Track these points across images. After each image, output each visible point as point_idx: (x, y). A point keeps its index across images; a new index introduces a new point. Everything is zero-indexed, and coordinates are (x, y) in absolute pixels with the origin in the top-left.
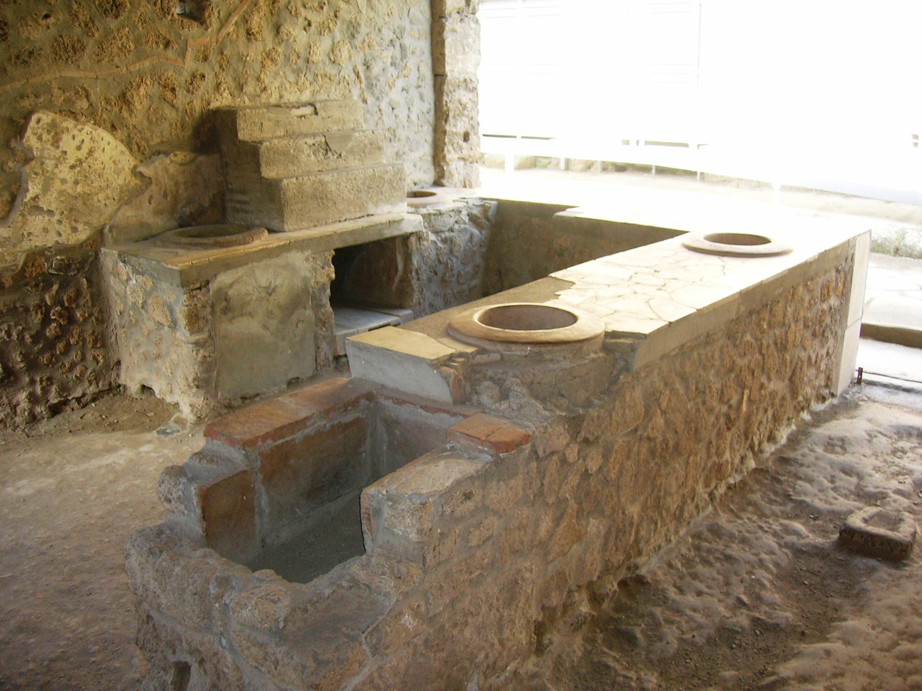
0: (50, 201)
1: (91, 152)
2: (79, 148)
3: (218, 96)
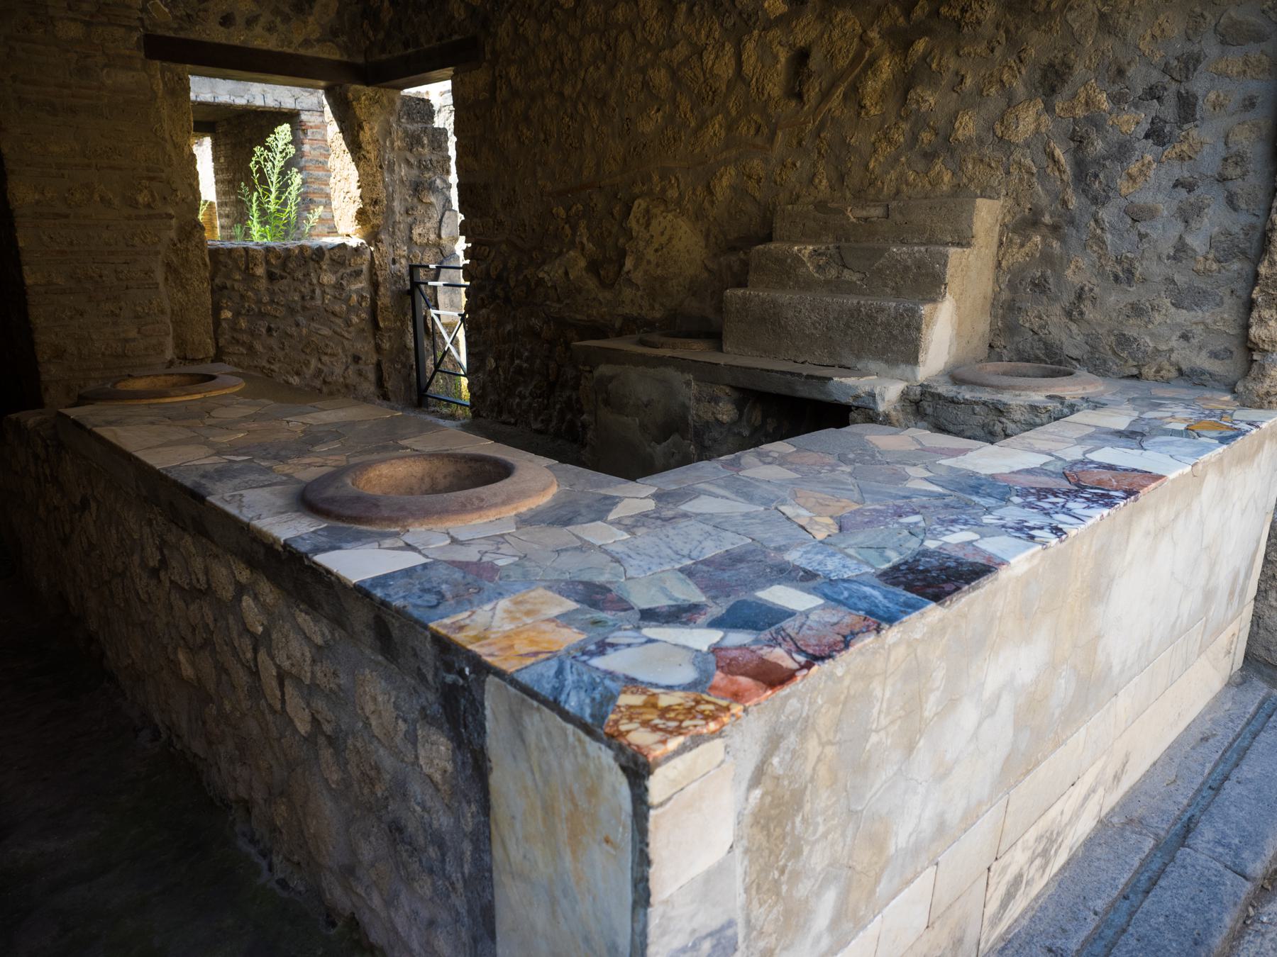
0: (638, 276)
1: (670, 239)
2: (662, 234)
3: (812, 189)
